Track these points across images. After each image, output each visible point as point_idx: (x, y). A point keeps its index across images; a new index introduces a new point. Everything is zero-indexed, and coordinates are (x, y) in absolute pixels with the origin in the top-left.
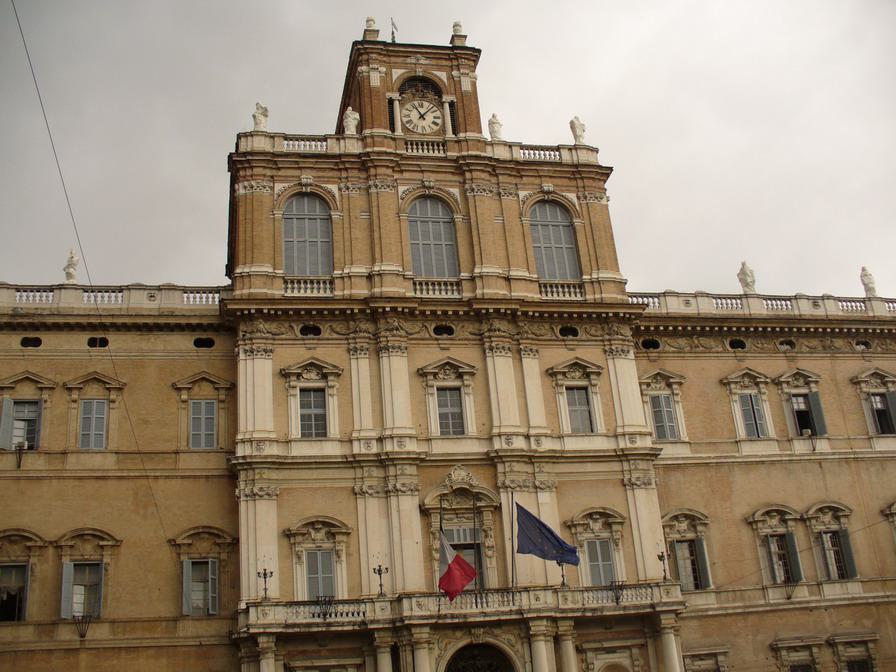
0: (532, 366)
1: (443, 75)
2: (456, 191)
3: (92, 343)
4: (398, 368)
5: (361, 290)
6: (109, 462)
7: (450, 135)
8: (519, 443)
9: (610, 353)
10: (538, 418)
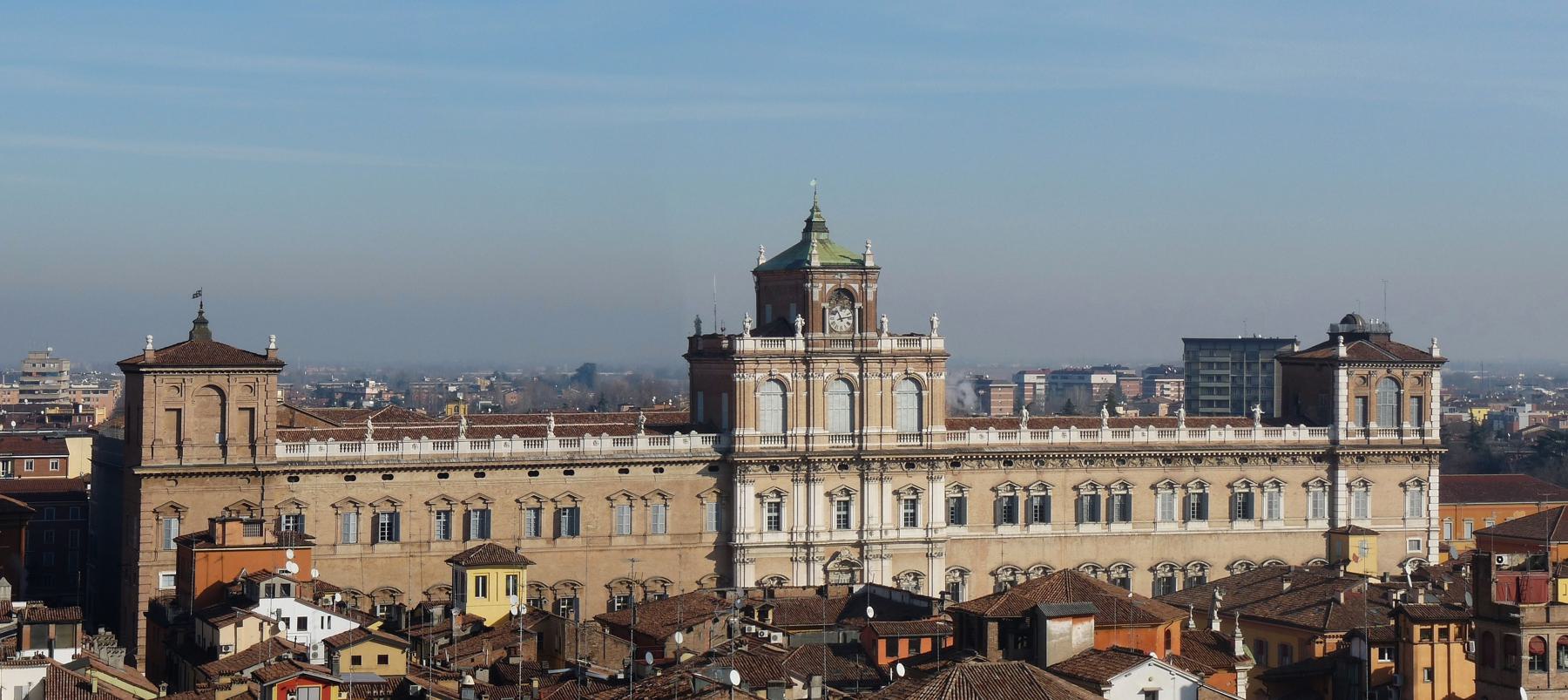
0: (888, 488)
1: (856, 287)
2: (856, 374)
3: (655, 471)
4: (819, 490)
5: (801, 445)
6: (666, 540)
7: (857, 335)
8: (876, 535)
9: (931, 479)
10: (888, 518)
